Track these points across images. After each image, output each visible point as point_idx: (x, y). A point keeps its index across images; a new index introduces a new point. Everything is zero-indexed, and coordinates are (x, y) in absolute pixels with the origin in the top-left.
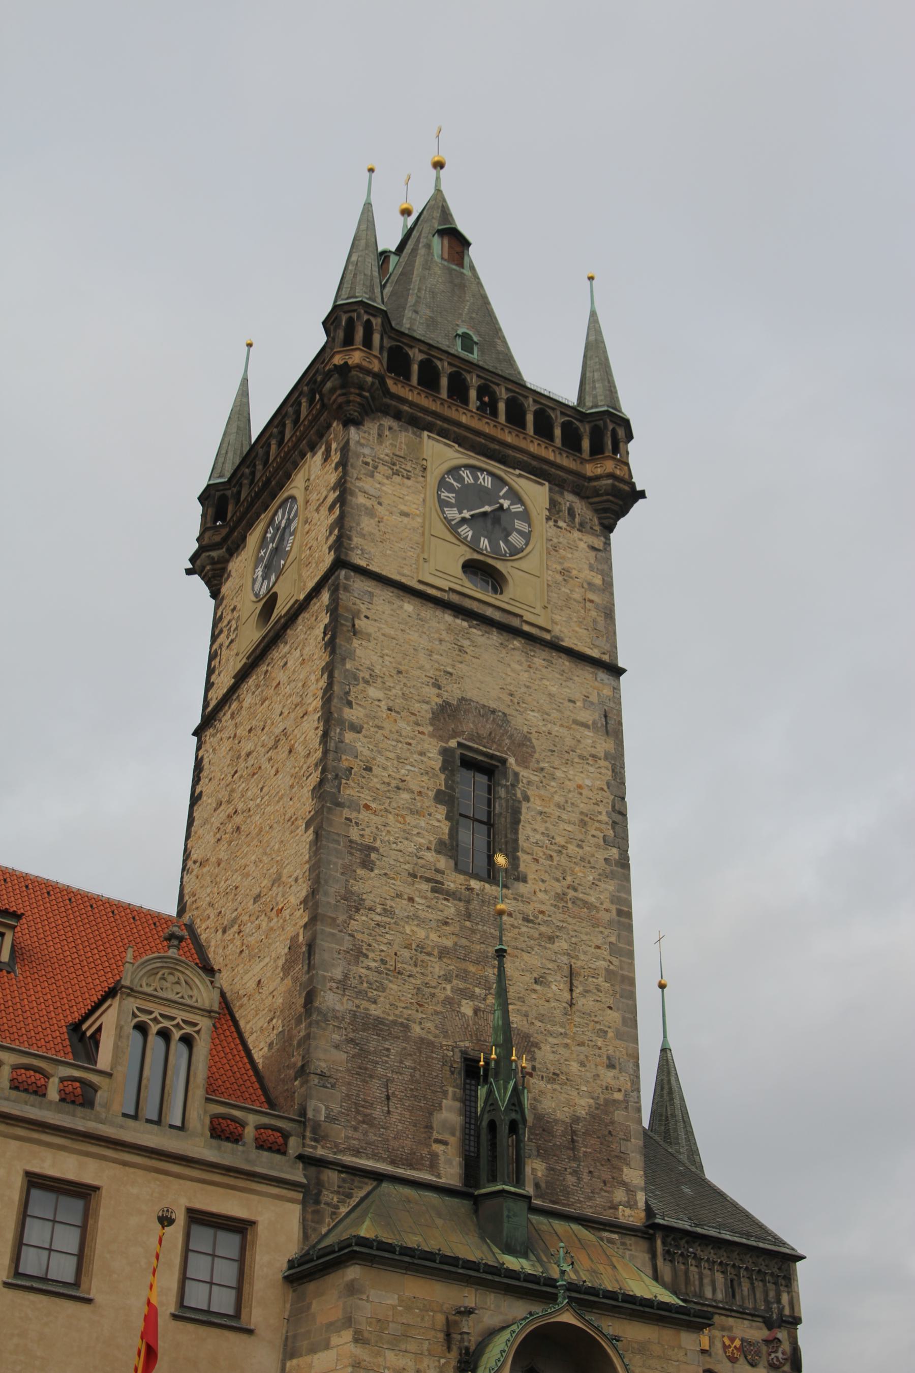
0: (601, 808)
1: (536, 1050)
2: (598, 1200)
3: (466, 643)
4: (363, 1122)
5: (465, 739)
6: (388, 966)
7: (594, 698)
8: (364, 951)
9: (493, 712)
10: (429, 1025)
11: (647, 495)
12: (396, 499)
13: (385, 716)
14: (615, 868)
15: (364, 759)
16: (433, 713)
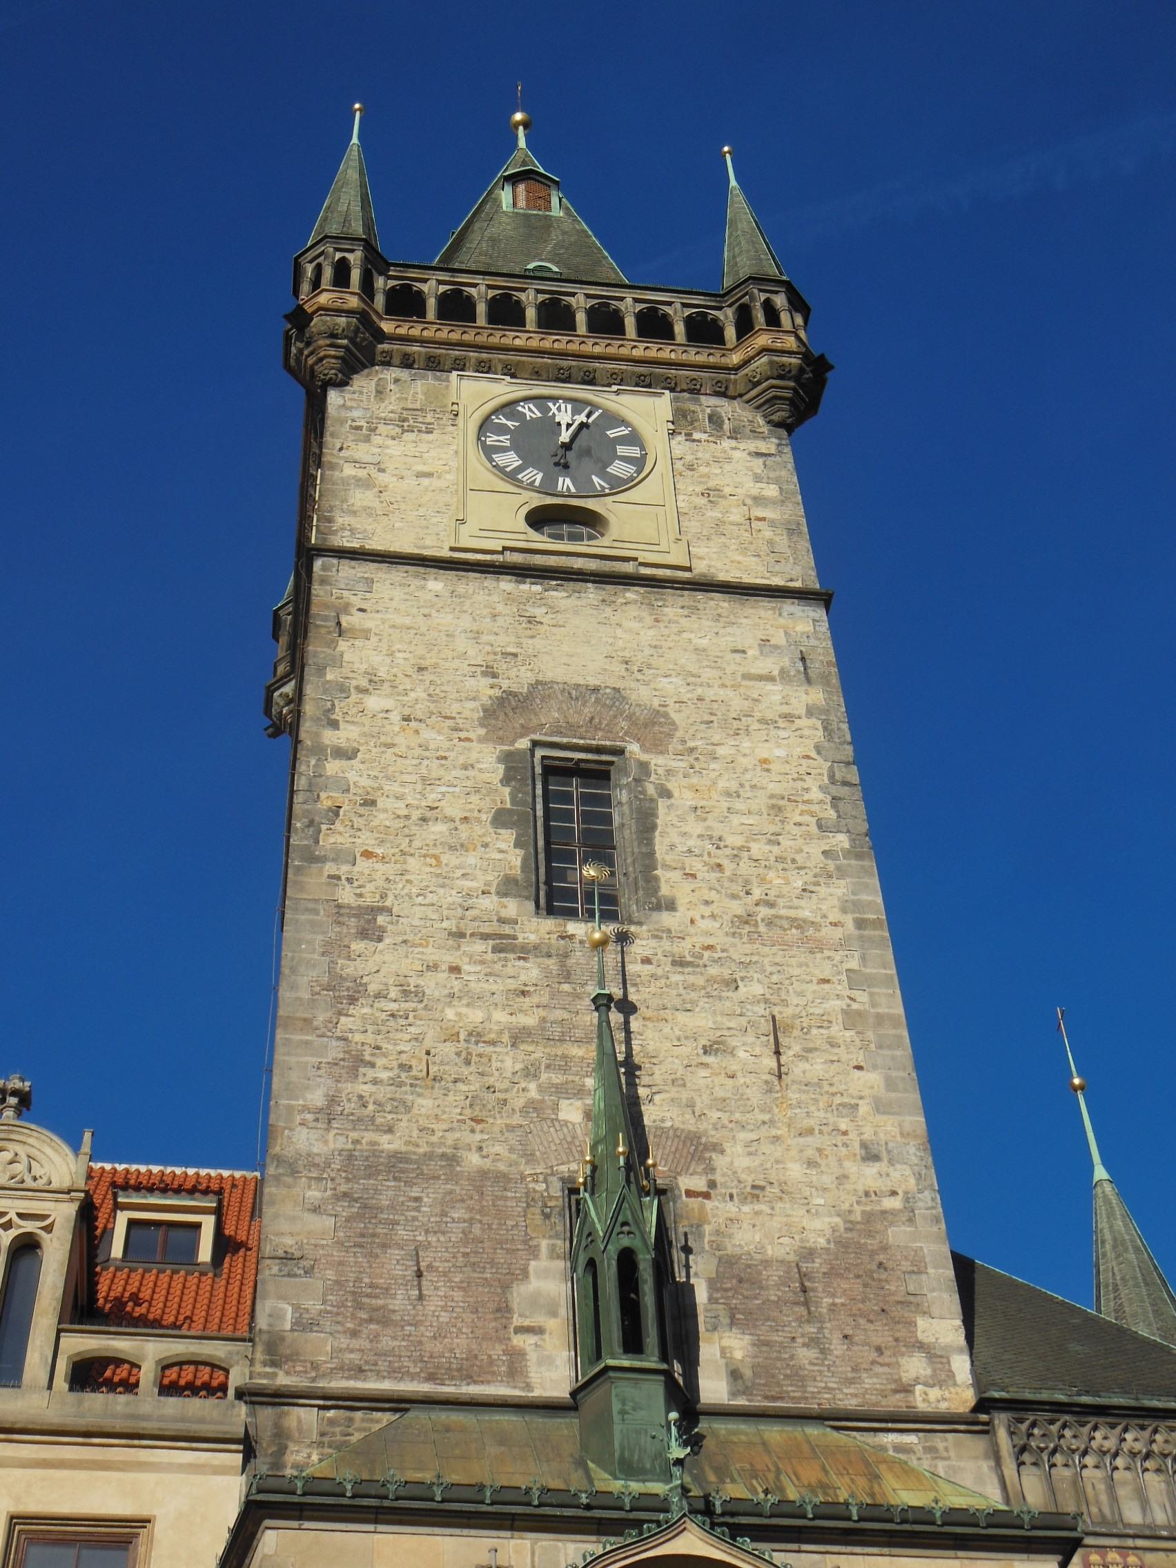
0: (809, 782)
1: (714, 1156)
2: (868, 1381)
3: (539, 612)
4: (371, 1320)
5: (545, 734)
6: (414, 1073)
7: (779, 639)
8: (367, 1058)
9: (596, 690)
10: (498, 1149)
11: (831, 360)
12: (410, 459)
13: (397, 729)
14: (845, 862)
15: (360, 791)
16: (485, 710)
